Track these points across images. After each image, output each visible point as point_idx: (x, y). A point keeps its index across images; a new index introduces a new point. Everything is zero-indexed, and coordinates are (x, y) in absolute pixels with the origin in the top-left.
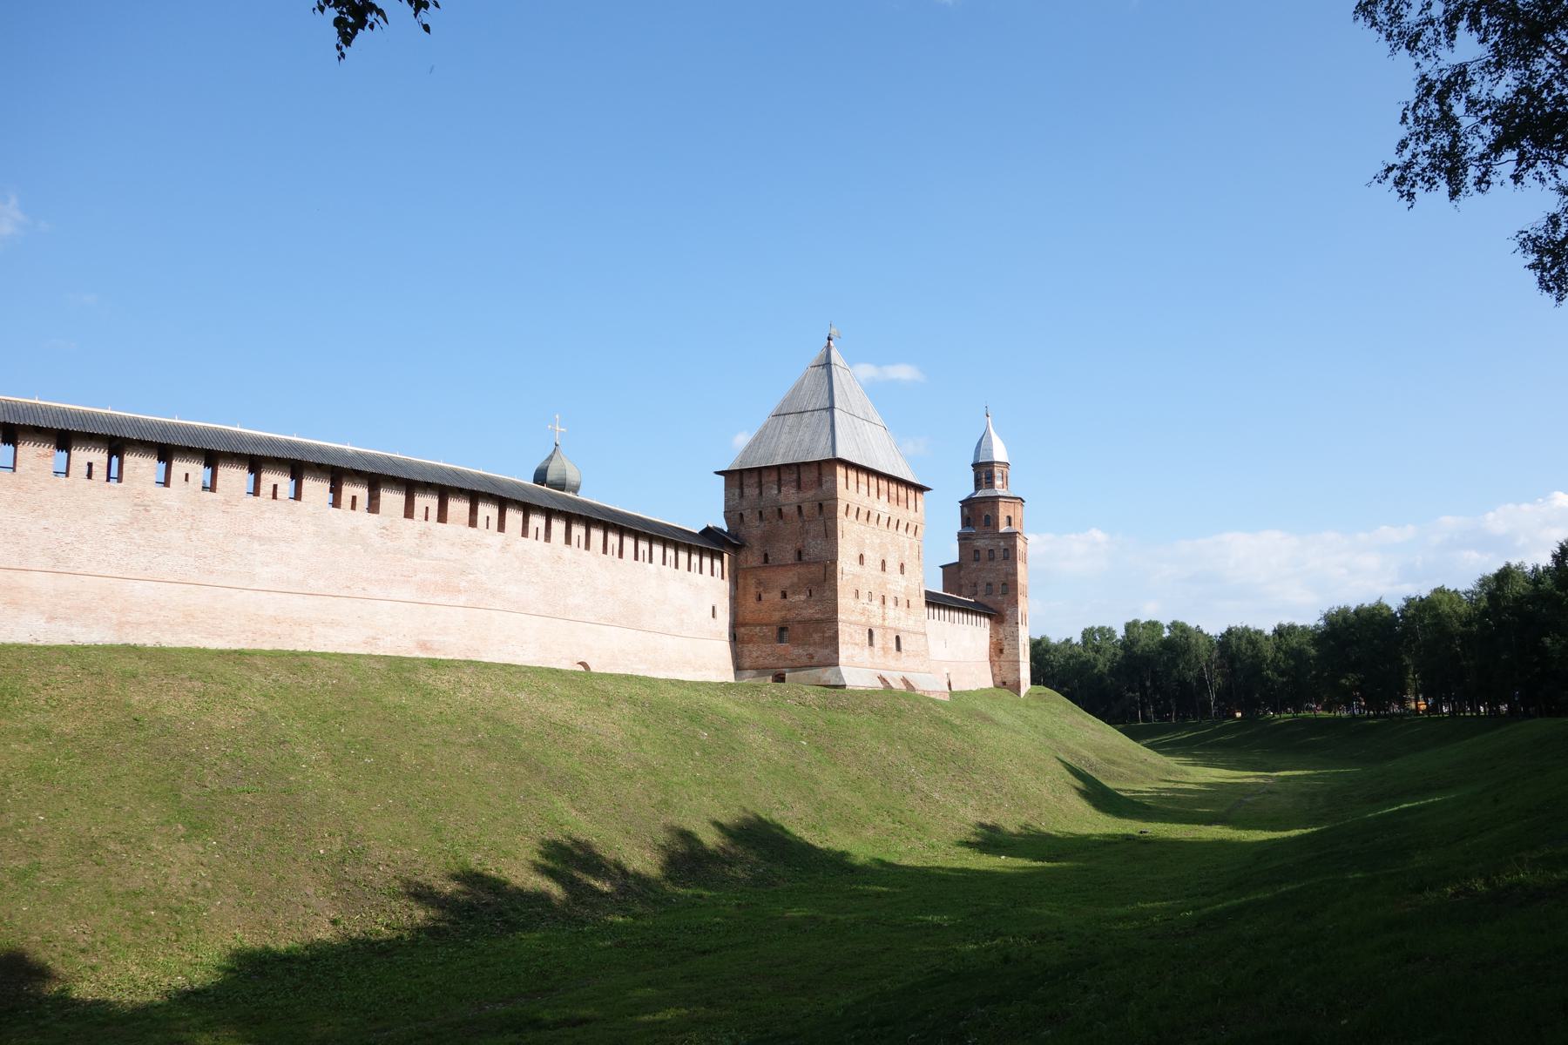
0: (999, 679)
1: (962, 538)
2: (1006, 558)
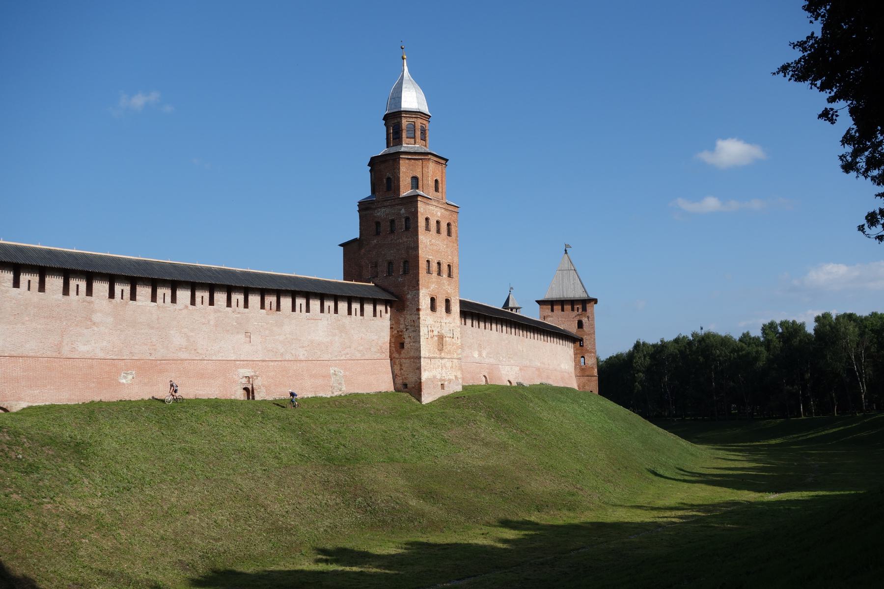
0: (399, 381)
1: (364, 207)
2: (407, 228)
